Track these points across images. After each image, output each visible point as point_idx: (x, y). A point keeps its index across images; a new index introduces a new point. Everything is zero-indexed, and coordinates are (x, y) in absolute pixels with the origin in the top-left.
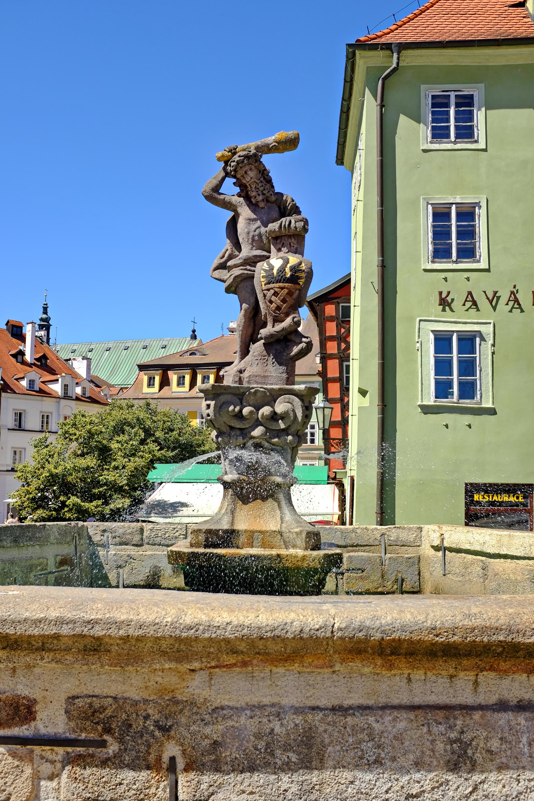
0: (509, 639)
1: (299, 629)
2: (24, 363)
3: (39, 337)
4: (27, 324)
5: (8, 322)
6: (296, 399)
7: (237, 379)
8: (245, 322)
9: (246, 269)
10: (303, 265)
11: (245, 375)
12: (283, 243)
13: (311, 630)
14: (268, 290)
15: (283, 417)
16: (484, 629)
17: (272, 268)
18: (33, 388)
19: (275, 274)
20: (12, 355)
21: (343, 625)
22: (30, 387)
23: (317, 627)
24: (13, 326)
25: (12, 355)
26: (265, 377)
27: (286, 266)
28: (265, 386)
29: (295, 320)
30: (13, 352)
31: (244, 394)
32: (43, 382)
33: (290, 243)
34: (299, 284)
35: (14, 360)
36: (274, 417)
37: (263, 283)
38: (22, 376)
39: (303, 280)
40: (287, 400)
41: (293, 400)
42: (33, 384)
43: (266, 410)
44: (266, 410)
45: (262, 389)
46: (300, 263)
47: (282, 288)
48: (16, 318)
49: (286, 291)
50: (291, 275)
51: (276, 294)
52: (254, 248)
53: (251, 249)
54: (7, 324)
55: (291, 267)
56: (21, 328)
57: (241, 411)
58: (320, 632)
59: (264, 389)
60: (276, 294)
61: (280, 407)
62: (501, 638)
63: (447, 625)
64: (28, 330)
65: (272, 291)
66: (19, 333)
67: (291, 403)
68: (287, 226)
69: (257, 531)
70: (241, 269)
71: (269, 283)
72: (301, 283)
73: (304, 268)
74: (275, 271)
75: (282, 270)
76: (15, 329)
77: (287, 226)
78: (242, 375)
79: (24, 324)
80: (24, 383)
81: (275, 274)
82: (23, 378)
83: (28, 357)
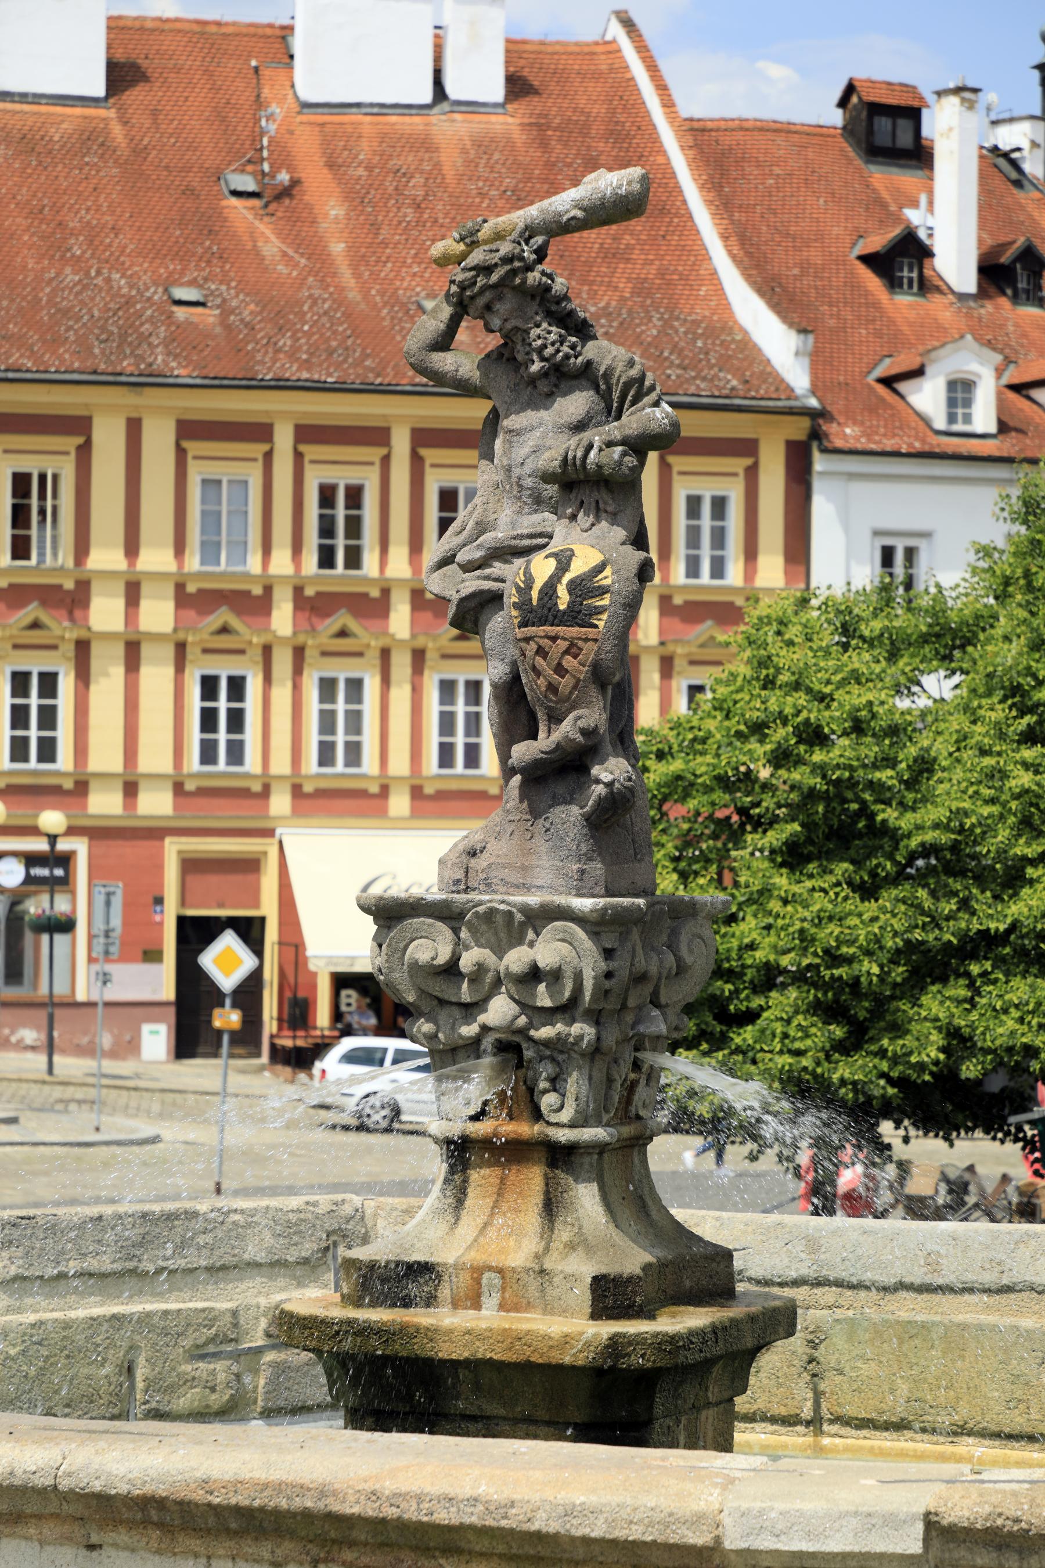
0: (321, 1505)
1: (8, 1470)
2: (925, 286)
3: (1006, 155)
4: (939, 94)
5: (850, 89)
6: (580, 933)
7: (460, 875)
8: (500, 713)
9: (487, 578)
10: (608, 571)
11: (480, 863)
12: (582, 502)
13: (25, 1472)
14: (527, 640)
15: (555, 976)
16: (279, 1487)
17: (529, 581)
18: (968, 419)
19: (535, 603)
20: (868, 260)
21: (73, 1469)
22: (952, 418)
23: (34, 1468)
24: (876, 109)
25: (868, 260)
26: (524, 868)
27: (559, 581)
28: (512, 899)
29: (581, 723)
30: (877, 242)
31: (461, 915)
32: (1017, 388)
33: (597, 502)
34: (596, 626)
35: (872, 281)
36: (534, 974)
37: (516, 621)
38: (913, 364)
39: (605, 617)
40: (560, 936)
41: (573, 935)
42: (968, 403)
43: (517, 959)
44: (517, 959)
45: (503, 907)
46: (600, 568)
47: (554, 639)
48: (887, 64)
49: (563, 645)
50: (571, 605)
51: (541, 651)
52: (526, 509)
53: (519, 513)
54: (843, 103)
55: (571, 582)
56: (913, 114)
57: (455, 959)
58: (38, 1475)
59: (509, 904)
60: (541, 651)
61: (547, 950)
62: (309, 1504)
63: (227, 1477)
64: (946, 127)
65: (533, 646)
66: (905, 140)
67: (570, 944)
68: (578, 462)
69: (490, 1269)
70: (479, 578)
71: (523, 624)
72: (601, 624)
73: (607, 582)
74: (535, 594)
75: (549, 590)
76: (883, 124)
77: (578, 462)
78: (473, 863)
79: (930, 98)
80: (927, 397)
81: (535, 603)
82: (919, 372)
83: (955, 261)
